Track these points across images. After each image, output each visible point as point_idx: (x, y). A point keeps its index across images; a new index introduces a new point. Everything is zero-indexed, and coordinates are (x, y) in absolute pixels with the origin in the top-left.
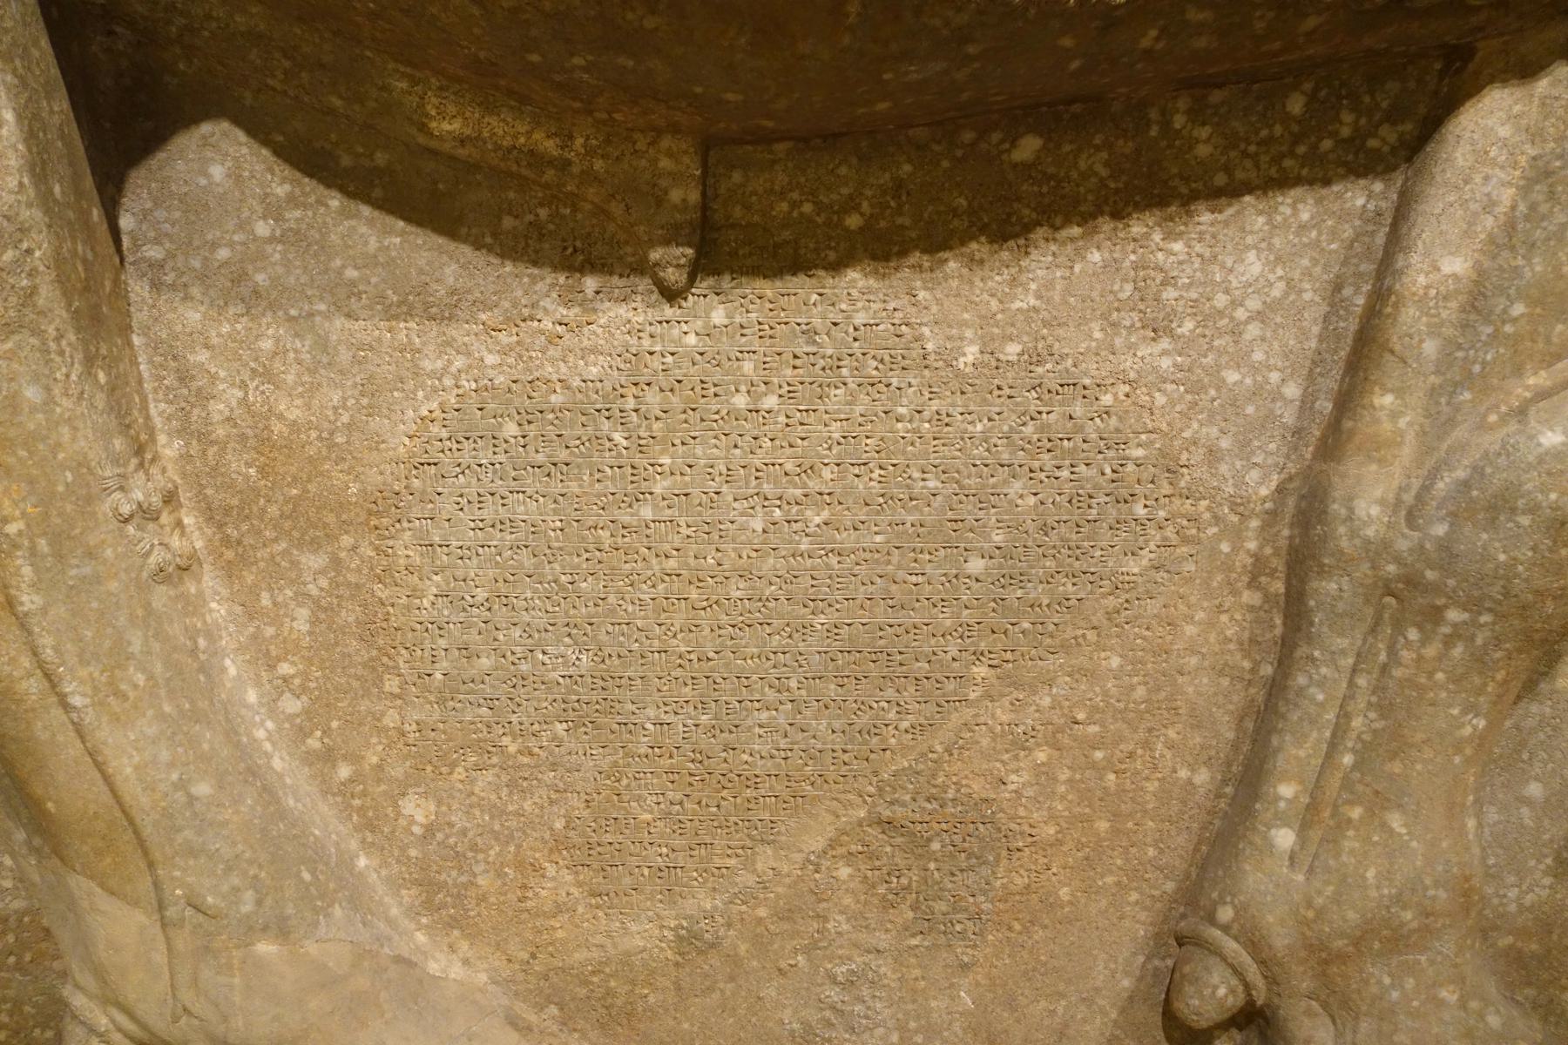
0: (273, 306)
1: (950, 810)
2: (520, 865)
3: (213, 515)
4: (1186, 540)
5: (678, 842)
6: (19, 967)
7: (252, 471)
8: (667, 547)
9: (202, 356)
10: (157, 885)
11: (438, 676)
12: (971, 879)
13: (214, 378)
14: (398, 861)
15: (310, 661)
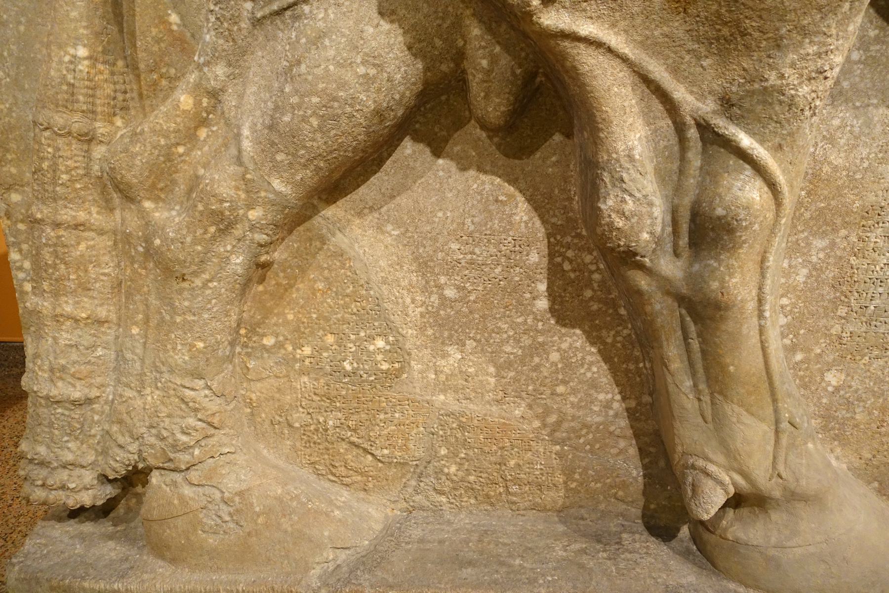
0: (846, 101)
6: (591, 451)
7: (803, 193)
10: (776, 411)
11: (872, 308)
14: (815, 405)
15: (799, 298)
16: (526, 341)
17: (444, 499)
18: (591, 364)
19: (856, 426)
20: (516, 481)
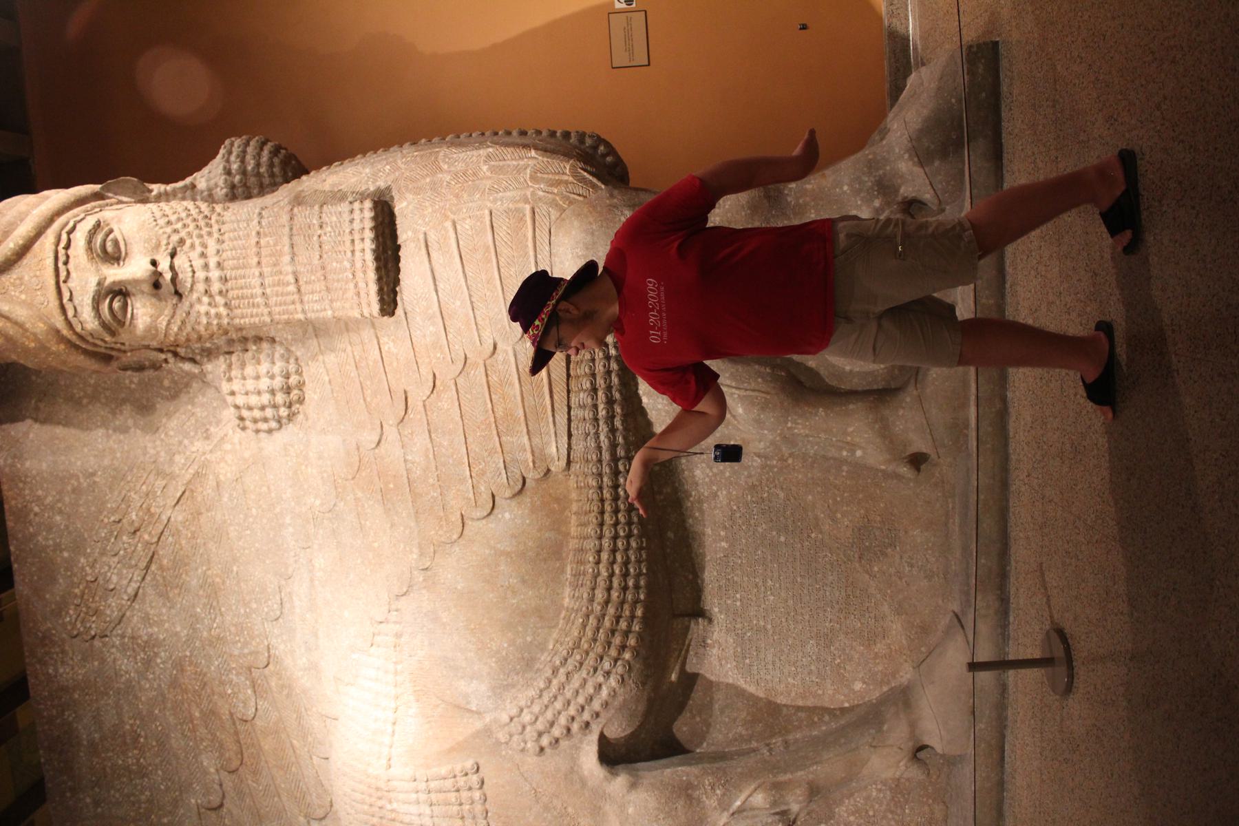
1: (855, 540)
3: (772, 735)
4: (774, 481)
5: (867, 615)
6: (909, 794)
8: (779, 622)
9: (730, 735)
12: (877, 533)
13: (736, 733)
18: (855, 801)
19: (886, 669)
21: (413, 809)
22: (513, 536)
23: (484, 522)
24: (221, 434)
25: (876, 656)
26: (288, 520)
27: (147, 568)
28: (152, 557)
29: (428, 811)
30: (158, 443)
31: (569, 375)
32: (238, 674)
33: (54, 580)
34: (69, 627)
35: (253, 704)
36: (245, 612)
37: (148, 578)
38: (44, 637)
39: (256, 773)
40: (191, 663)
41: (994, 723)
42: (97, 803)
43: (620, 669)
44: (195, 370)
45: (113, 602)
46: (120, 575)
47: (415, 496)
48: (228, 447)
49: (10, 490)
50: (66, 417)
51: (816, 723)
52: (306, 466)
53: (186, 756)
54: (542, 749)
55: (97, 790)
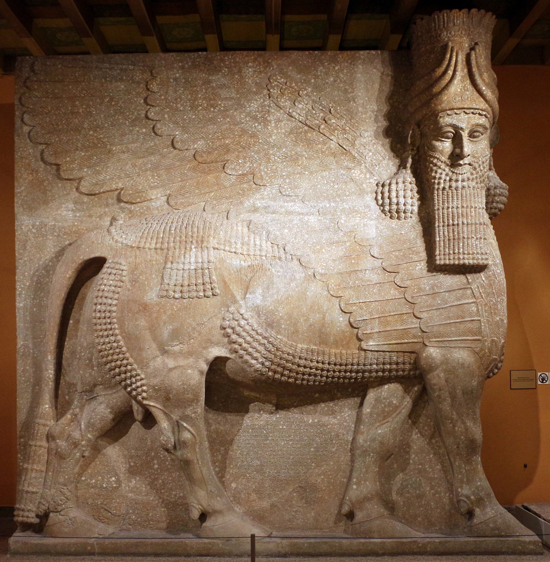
2: (248, 494)
16: (153, 477)
17: (131, 527)
18: (170, 483)
20: (152, 520)
21: (193, 260)
22: (332, 322)
23: (339, 307)
24: (375, 173)
25: (249, 494)
26: (333, 204)
27: (306, 125)
28: (312, 128)
29: (192, 268)
30: (370, 139)
31: (404, 352)
32: (250, 167)
33: (299, 73)
34: (274, 78)
35: (234, 173)
36: (284, 176)
37: (300, 124)
38: (268, 63)
39: (194, 169)
40: (255, 142)
41: (221, 551)
42: (175, 79)
43: (264, 370)
44: (409, 165)
45: (288, 104)
46: (302, 109)
47: (350, 273)
48: (368, 176)
49: (347, 56)
50: (384, 90)
51: (215, 464)
52: (360, 217)
53: (203, 132)
54: (224, 329)
55: (183, 81)
